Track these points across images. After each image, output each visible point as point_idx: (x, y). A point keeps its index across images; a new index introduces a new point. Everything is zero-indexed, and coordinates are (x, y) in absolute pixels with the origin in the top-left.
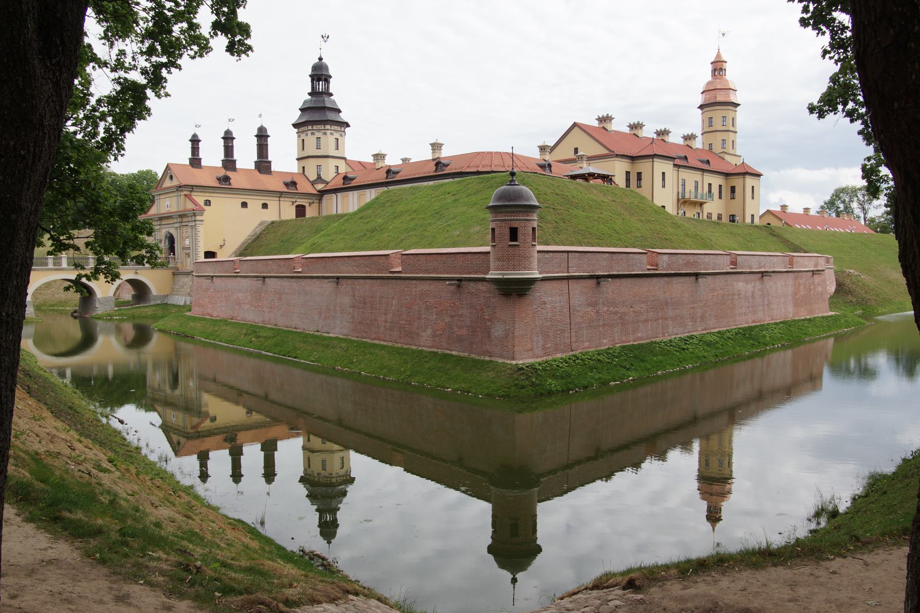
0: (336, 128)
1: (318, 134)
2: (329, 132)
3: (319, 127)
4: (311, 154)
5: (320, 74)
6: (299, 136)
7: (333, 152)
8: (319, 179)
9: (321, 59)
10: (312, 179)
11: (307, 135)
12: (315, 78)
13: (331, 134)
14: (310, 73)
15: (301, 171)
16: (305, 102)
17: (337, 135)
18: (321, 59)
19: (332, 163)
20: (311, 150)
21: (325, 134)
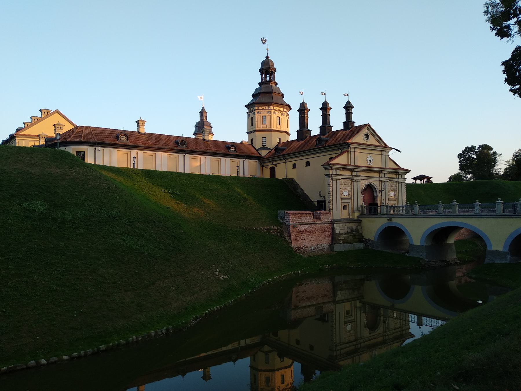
1: (264, 113)
2: (272, 111)
3: (263, 107)
4: (257, 129)
5: (267, 69)
6: (249, 116)
7: (275, 127)
8: (264, 148)
9: (267, 57)
10: (257, 148)
11: (254, 114)
12: (264, 71)
13: (275, 113)
14: (259, 67)
15: (250, 143)
16: (257, 90)
17: (279, 114)
18: (267, 57)
20: (258, 125)
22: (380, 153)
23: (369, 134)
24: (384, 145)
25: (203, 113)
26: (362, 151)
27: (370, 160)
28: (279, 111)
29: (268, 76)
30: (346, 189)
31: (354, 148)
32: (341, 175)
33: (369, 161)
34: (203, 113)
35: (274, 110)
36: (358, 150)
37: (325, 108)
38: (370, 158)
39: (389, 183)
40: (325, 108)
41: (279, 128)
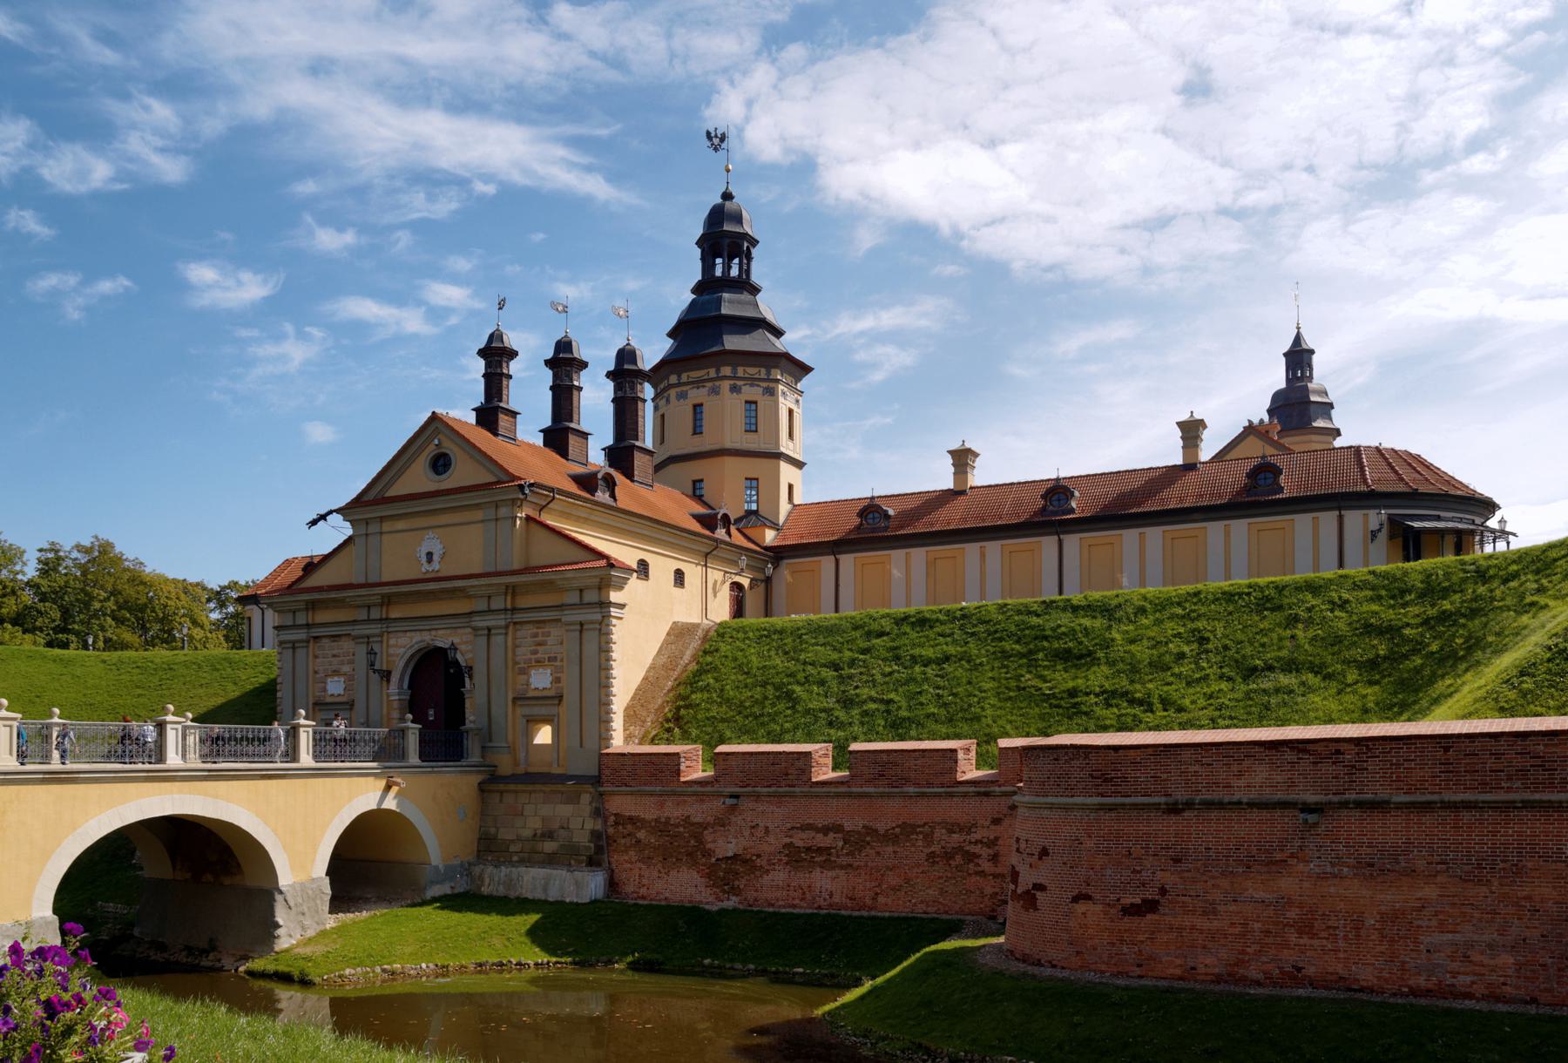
0: (695, 374)
2: (673, 393)
19: (734, 469)
21: (771, 392)
22: (479, 515)
23: (450, 447)
24: (505, 478)
25: (1298, 358)
26: (400, 525)
27: (430, 555)
28: (698, 383)
29: (736, 261)
30: (336, 673)
31: (367, 522)
32: (308, 626)
33: (424, 559)
34: (1298, 358)
35: (679, 385)
36: (386, 527)
37: (564, 363)
38: (431, 542)
39: (527, 631)
40: (564, 363)
41: (706, 443)
